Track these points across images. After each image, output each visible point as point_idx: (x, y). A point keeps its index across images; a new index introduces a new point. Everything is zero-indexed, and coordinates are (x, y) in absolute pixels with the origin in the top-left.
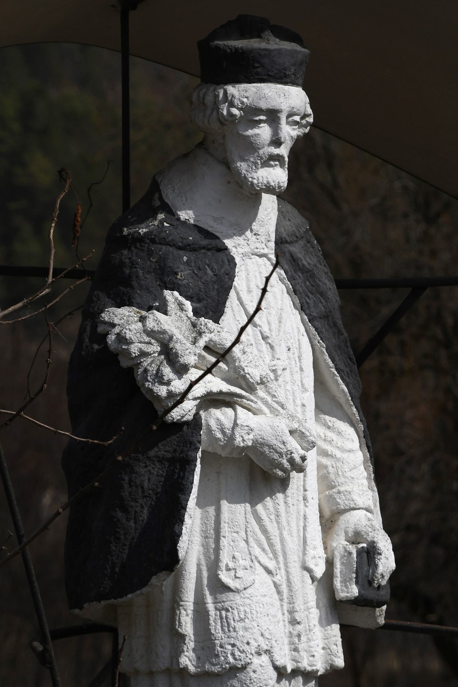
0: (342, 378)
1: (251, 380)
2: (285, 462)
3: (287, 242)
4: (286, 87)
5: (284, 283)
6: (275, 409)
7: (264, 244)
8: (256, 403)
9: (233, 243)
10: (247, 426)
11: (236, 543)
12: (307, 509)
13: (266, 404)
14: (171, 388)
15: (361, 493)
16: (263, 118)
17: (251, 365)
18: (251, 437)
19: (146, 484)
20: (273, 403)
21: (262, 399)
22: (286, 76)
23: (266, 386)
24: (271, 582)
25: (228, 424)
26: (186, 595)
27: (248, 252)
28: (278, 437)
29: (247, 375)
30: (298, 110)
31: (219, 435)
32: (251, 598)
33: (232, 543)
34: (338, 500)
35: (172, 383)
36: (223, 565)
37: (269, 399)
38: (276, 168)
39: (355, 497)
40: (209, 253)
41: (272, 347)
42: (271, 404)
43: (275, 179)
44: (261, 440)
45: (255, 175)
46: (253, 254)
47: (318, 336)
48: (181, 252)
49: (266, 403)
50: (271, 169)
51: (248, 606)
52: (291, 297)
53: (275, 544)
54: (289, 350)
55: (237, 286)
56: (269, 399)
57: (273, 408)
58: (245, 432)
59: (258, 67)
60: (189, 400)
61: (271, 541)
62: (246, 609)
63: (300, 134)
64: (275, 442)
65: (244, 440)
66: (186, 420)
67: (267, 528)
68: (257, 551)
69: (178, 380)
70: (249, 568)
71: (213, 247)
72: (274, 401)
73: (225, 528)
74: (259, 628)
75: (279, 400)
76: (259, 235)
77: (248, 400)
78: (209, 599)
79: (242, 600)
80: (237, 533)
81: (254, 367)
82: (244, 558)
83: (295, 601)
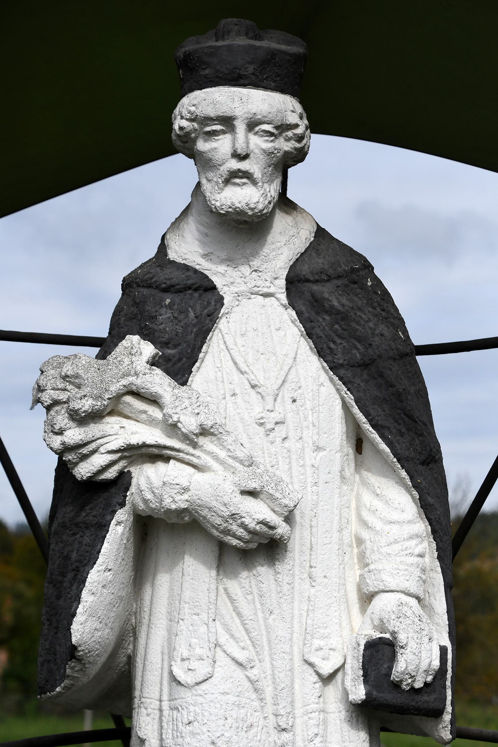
0: (382, 436)
2: (234, 527)
3: (308, 281)
8: (198, 457)
9: (224, 281)
11: (195, 628)
12: (313, 591)
13: (216, 459)
14: (66, 440)
15: (394, 572)
16: (218, 127)
17: (187, 413)
18: (186, 497)
19: (74, 556)
20: (228, 458)
22: (240, 77)
23: (219, 439)
24: (244, 677)
25: (157, 483)
26: (147, 690)
27: (244, 291)
28: (218, 498)
29: (179, 424)
30: (265, 117)
31: (149, 496)
32: (205, 696)
33: (191, 628)
34: (368, 581)
35: (66, 433)
36: (177, 655)
37: (222, 454)
38: (244, 187)
39: (384, 577)
40: (196, 295)
42: (223, 460)
44: (198, 501)
45: (218, 197)
46: (252, 294)
47: (343, 386)
48: (166, 295)
49: (216, 458)
50: (238, 189)
51: (200, 706)
53: (251, 630)
55: (223, 329)
56: (222, 454)
58: (176, 491)
61: (246, 626)
62: (197, 708)
64: (214, 503)
65: (174, 501)
66: (106, 478)
67: (241, 610)
68: (223, 638)
70: (205, 658)
72: (229, 456)
73: (186, 609)
74: (209, 734)
75: (234, 454)
76: (261, 272)
77: (187, 454)
78: (165, 697)
79: (194, 698)
80: (198, 614)
81: (190, 415)
82: (202, 646)
83: (279, 702)
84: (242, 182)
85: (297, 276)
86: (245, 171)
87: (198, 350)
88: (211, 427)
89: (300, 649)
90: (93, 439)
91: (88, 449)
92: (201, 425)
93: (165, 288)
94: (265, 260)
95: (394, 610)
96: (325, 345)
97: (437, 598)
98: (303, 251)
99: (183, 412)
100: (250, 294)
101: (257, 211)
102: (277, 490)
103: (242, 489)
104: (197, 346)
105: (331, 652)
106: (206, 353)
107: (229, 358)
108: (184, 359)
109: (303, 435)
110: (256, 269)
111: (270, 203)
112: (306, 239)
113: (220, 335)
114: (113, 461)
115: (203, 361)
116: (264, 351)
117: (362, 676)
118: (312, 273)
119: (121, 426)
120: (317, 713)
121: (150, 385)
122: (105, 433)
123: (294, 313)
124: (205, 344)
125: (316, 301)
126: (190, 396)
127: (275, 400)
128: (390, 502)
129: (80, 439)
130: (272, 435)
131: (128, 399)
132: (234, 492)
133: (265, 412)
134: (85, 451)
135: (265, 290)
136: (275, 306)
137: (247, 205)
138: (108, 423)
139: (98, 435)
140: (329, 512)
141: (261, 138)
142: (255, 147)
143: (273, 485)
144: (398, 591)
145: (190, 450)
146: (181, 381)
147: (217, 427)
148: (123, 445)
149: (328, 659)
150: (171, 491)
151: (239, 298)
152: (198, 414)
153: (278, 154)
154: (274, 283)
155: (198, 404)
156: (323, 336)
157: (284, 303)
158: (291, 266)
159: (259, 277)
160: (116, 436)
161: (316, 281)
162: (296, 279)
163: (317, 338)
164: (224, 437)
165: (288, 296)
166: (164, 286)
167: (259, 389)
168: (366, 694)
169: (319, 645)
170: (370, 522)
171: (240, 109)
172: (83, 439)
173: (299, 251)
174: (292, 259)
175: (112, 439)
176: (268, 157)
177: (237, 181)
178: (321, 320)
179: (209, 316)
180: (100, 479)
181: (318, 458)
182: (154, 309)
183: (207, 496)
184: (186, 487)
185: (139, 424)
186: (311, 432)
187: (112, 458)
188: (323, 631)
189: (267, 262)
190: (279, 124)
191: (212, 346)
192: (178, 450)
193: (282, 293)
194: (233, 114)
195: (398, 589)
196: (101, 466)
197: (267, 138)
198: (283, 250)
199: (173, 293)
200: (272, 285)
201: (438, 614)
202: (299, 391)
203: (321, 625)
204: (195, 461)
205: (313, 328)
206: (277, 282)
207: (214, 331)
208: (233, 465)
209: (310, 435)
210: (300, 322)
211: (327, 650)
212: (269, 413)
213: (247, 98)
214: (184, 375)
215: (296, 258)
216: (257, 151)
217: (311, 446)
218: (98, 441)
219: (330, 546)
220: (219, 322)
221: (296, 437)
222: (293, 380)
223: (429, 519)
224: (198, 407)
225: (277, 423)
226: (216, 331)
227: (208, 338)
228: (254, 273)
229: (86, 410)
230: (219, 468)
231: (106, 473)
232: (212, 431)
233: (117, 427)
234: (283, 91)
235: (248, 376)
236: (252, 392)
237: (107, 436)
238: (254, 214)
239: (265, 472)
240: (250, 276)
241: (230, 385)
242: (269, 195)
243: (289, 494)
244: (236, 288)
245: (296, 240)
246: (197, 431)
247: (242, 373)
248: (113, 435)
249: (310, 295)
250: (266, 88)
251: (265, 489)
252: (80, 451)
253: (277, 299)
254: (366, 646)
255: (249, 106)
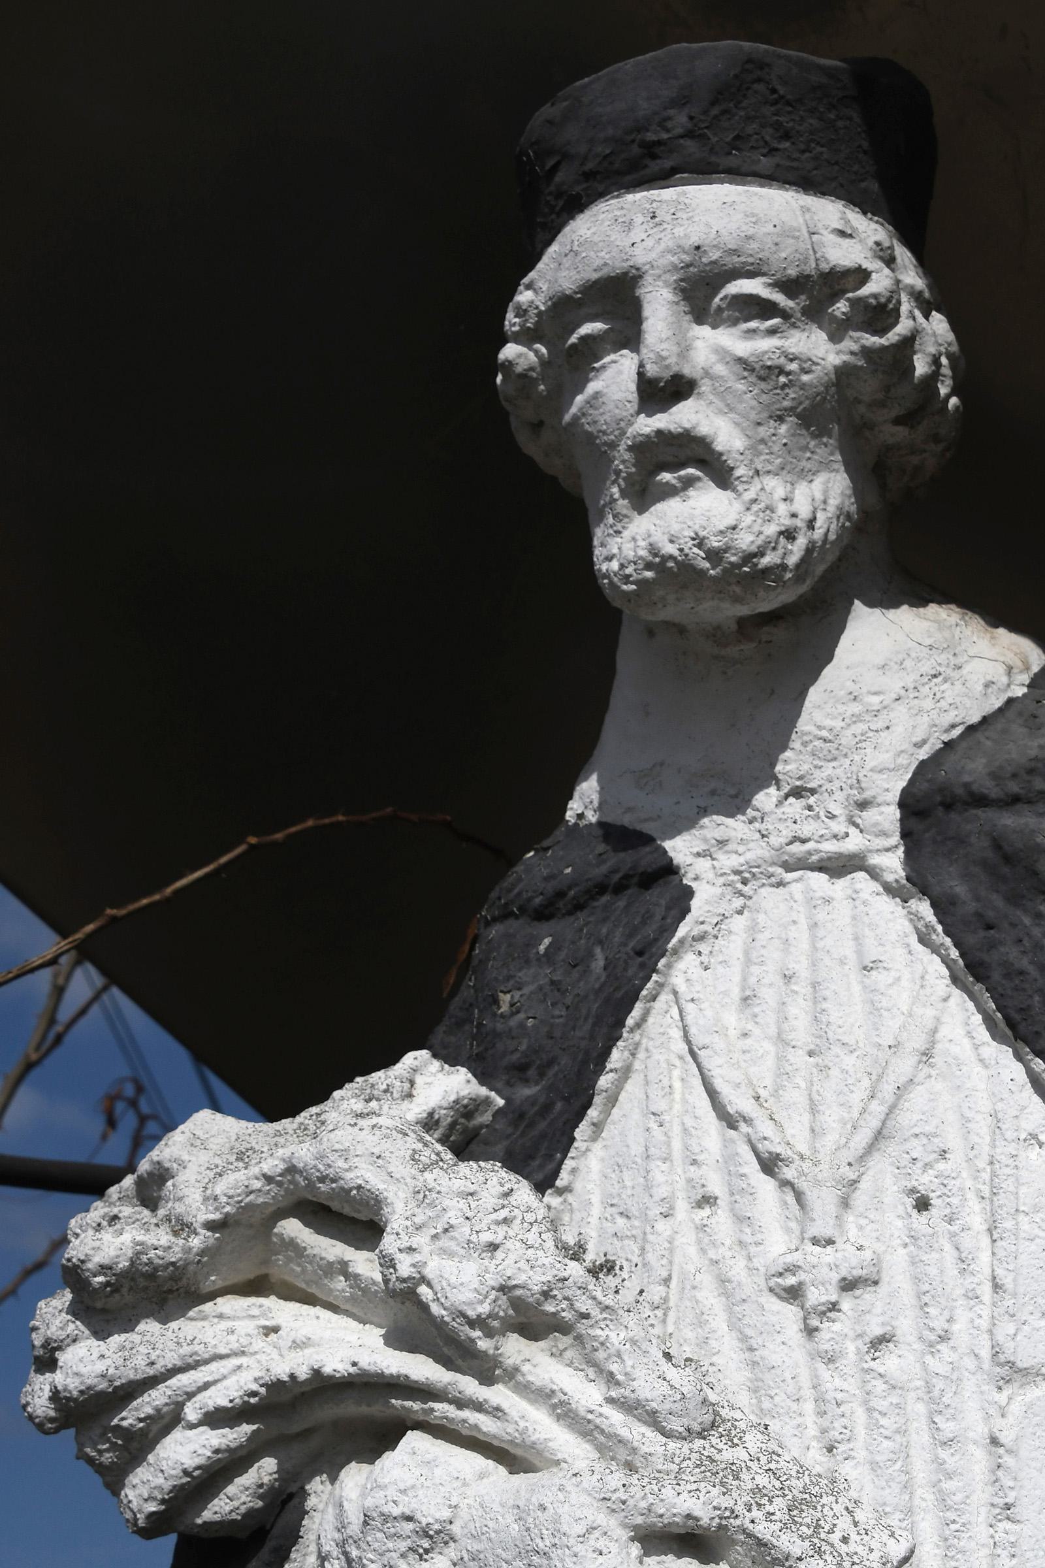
1: (435, 1309)
3: (980, 801)
4: (668, 194)
5: (935, 949)
6: (609, 1436)
7: (842, 819)
8: (497, 1412)
9: (698, 842)
10: (409, 1519)
17: (452, 1245)
20: (607, 1410)
21: (544, 1396)
23: (579, 1338)
27: (760, 862)
29: (423, 1290)
35: (63, 1358)
38: (691, 492)
41: (799, 1196)
42: (590, 1416)
43: (675, 528)
46: (788, 867)
49: (564, 1412)
52: (972, 996)
54: (923, 1204)
55: (682, 988)
57: (602, 1431)
58: (403, 1545)
59: (555, 168)
60: (192, 1426)
63: (846, 358)
66: (217, 1518)
69: (93, 1342)
71: (627, 877)
72: (611, 1401)
75: (627, 1393)
76: (813, 791)
77: (460, 1403)
81: (462, 1252)
84: (680, 478)
85: (941, 790)
86: (680, 435)
87: (596, 1065)
88: (546, 1295)
90: (151, 1372)
91: (137, 1409)
92: (502, 1289)
93: (541, 906)
94: (825, 752)
96: (1037, 998)
98: (975, 719)
99: (439, 1244)
100: (780, 870)
101: (733, 559)
102: (790, 1524)
103: (639, 1520)
104: (595, 1054)
106: (626, 1072)
107: (697, 1082)
108: (559, 1106)
109: (955, 1327)
110: (798, 783)
111: (789, 535)
112: (987, 686)
113: (675, 1012)
114: (229, 1450)
115: (613, 1100)
116: (818, 1041)
118: (994, 776)
119: (268, 1323)
121: (341, 1163)
122: (199, 1348)
123: (924, 908)
124: (620, 1043)
125: (1007, 859)
126: (472, 1188)
127: (845, 1203)
129: (99, 1372)
130: (829, 1330)
131: (292, 1228)
132: (596, 1533)
133: (809, 1247)
134: (130, 1417)
135: (830, 847)
136: (864, 895)
137: (700, 542)
138: (221, 1316)
139: (171, 1359)
141: (733, 330)
142: (713, 358)
143: (780, 1503)
145: (469, 1386)
146: (540, 1176)
147: (568, 1293)
148: (255, 1387)
150: (390, 1545)
151: (746, 889)
152: (493, 1247)
153: (805, 378)
154: (859, 821)
155: (503, 1214)
156: (1031, 969)
157: (890, 878)
158: (923, 763)
159: (810, 808)
160: (243, 1360)
161: (1013, 801)
162: (939, 798)
163: (1007, 976)
164: (599, 1332)
165: (910, 858)
166: (538, 900)
167: (785, 1169)
171: (650, 243)
172: (111, 1371)
173: (958, 720)
174: (924, 742)
175: (224, 1371)
176: (763, 385)
177: (666, 477)
178: (1027, 921)
179: (640, 953)
180: (199, 1521)
181: (1015, 1408)
182: (505, 971)
183: (504, 1555)
184: (437, 1527)
185: (334, 1317)
186: (986, 1313)
187: (224, 1441)
189: (835, 759)
190: (792, 272)
191: (647, 1050)
192: (425, 1392)
193: (888, 850)
194: (625, 265)
196: (186, 1473)
197: (753, 324)
198: (892, 715)
199: (564, 915)
200: (852, 830)
202: (941, 1166)
204: (487, 1425)
205: (992, 945)
206: (869, 816)
207: (654, 998)
208: (624, 1433)
209: (984, 1324)
210: (947, 933)
212: (817, 1249)
213: (672, 211)
214: (550, 1157)
215: (946, 738)
216: (720, 369)
217: (987, 1365)
218: (173, 1382)
220: (669, 966)
221: (926, 1333)
222: (917, 1130)
224: (498, 1223)
225: (848, 1285)
226: (665, 997)
227: (630, 1022)
228: (791, 800)
229: (106, 1261)
230: (577, 1451)
231: (216, 1501)
232: (550, 1308)
233: (246, 1327)
234: (808, 184)
235: (750, 1130)
236: (765, 1185)
237: (207, 1362)
238: (725, 571)
239: (763, 1459)
240: (779, 811)
241: (692, 1168)
242: (782, 509)
243: (845, 1540)
244: (734, 856)
245: (946, 686)
246: (484, 1309)
247: (729, 1120)
248: (227, 1356)
249: (986, 844)
250: (738, 174)
251: (738, 1522)
252: (115, 1421)
253: (874, 873)
255: (679, 231)
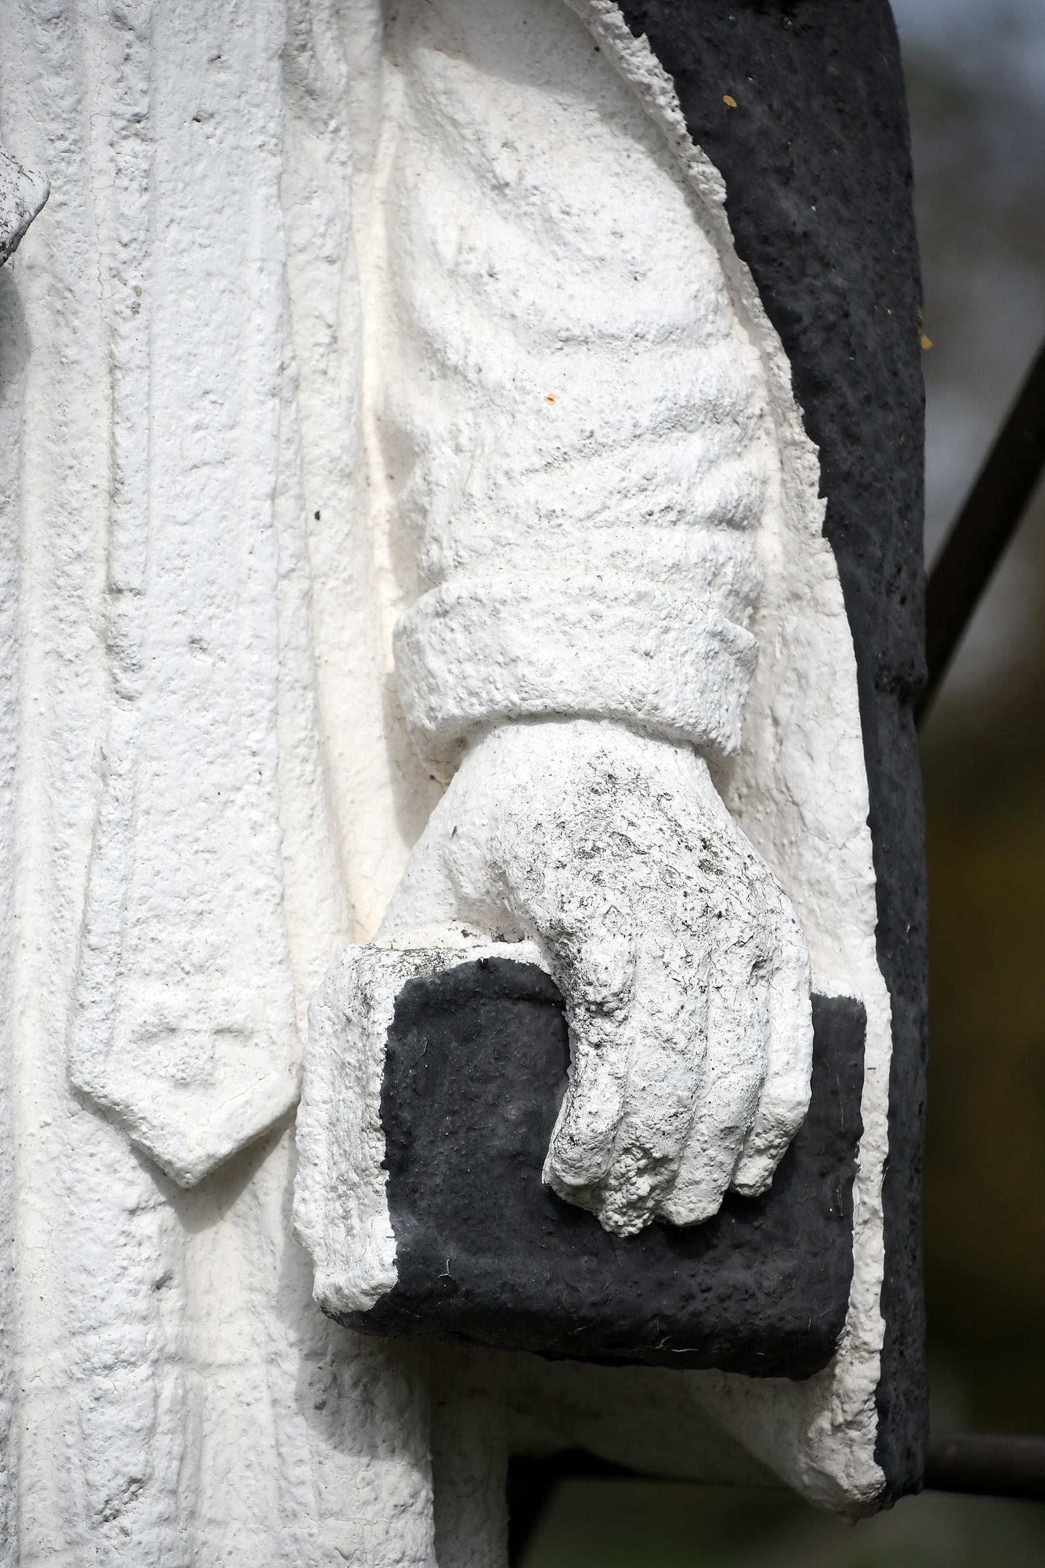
34: (434, 662)
89: (53, 1033)
95: (567, 811)
97: (820, 747)
105: (226, 1047)
117: (384, 1166)
120: (144, 1370)
128: (566, 226)
140: (218, 284)
144: (593, 716)
149: (207, 1084)
168: (403, 1261)
169: (159, 1009)
170: (455, 340)
188: (181, 936)
195: (596, 704)
201: (822, 834)
203: (174, 905)
211: (205, 1039)
219: (222, 473)
223: (781, 319)
254: (401, 1006)
